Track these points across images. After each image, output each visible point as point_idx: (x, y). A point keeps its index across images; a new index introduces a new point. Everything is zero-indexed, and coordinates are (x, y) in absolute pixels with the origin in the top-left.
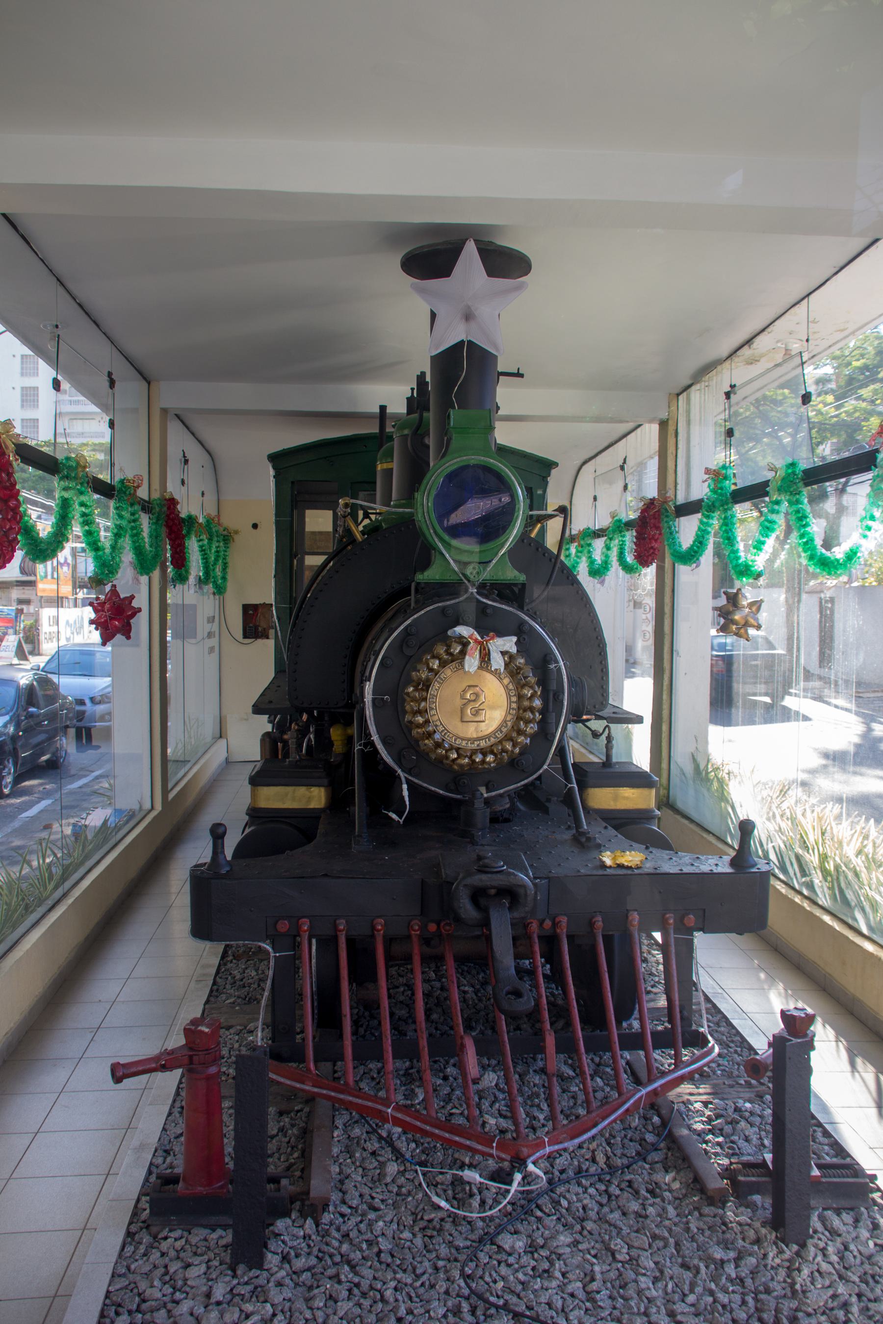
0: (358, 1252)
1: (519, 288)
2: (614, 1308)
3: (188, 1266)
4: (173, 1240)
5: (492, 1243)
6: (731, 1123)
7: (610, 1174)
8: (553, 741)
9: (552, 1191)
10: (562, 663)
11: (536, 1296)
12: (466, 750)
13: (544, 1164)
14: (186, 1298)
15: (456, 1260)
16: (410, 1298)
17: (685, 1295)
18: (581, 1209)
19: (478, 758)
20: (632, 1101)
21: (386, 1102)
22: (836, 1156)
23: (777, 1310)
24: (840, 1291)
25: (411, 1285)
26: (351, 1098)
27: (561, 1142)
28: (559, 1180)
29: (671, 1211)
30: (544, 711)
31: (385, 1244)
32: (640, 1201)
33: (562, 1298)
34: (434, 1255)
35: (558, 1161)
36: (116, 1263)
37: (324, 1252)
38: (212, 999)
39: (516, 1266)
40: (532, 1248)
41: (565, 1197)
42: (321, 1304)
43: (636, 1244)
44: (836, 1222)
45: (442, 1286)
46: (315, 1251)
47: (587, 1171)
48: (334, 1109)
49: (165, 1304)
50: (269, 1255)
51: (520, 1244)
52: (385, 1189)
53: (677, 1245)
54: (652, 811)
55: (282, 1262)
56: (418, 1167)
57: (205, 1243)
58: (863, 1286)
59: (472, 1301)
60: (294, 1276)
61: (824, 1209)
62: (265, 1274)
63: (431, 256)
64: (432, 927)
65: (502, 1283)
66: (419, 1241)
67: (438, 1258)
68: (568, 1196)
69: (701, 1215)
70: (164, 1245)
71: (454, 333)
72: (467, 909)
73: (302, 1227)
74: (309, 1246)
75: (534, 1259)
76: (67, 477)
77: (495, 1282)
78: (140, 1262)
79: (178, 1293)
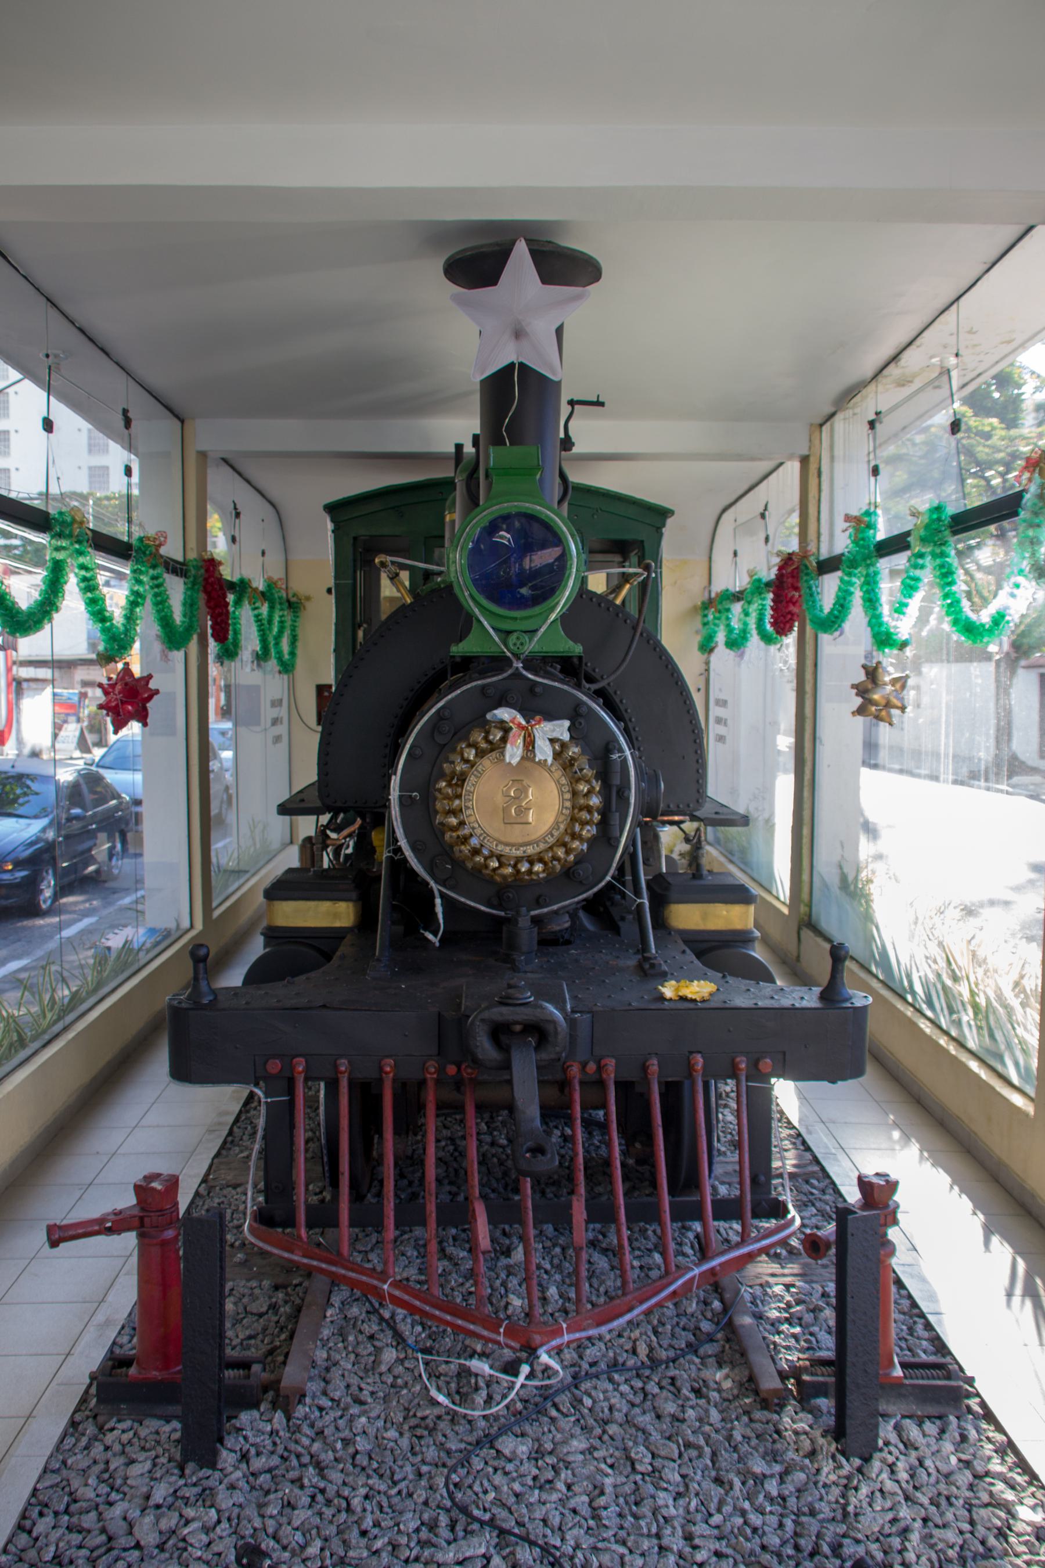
0: (330, 1453)
1: (578, 297)
2: (622, 1527)
3: (132, 1462)
4: (120, 1431)
5: (492, 1447)
6: (813, 1311)
7: (652, 1369)
8: (617, 848)
9: (576, 1387)
10: (628, 753)
11: (529, 1511)
12: (509, 858)
13: (569, 1355)
14: (123, 1500)
15: (444, 1465)
16: (381, 1508)
17: (710, 1515)
18: (606, 1410)
19: (524, 867)
20: (680, 1282)
21: (383, 1276)
22: (935, 1354)
23: (819, 1535)
24: (901, 1514)
25: (385, 1493)
26: (343, 1272)
27: (584, 1330)
28: (587, 1373)
29: (715, 1415)
30: (605, 812)
31: (362, 1444)
32: (680, 1402)
33: (562, 1514)
34: (419, 1458)
35: (588, 1351)
36: (51, 1456)
37: (290, 1451)
38: (224, 1152)
39: (515, 1474)
40: (537, 1455)
41: (590, 1395)
42: (275, 1512)
43: (663, 1453)
44: (913, 1432)
45: (420, 1495)
46: (280, 1449)
47: (623, 1364)
48: (333, 1284)
49: (97, 1505)
50: (224, 1453)
51: (523, 1449)
52: (378, 1379)
53: (714, 1454)
54: (750, 932)
55: (240, 1461)
56: (420, 1355)
57: (155, 1436)
58: (933, 1509)
59: (453, 1514)
60: (251, 1478)
61: (904, 1417)
62: (217, 1475)
63: (477, 262)
64: (451, 1070)
65: (493, 1494)
66: (405, 1442)
67: (423, 1462)
68: (593, 1393)
69: (751, 1420)
70: (109, 1438)
71: (507, 355)
72: (485, 1048)
73: (270, 1421)
74: (275, 1444)
75: (537, 1467)
76: (60, 536)
77: (485, 1492)
78: (79, 1456)
79: (114, 1494)
